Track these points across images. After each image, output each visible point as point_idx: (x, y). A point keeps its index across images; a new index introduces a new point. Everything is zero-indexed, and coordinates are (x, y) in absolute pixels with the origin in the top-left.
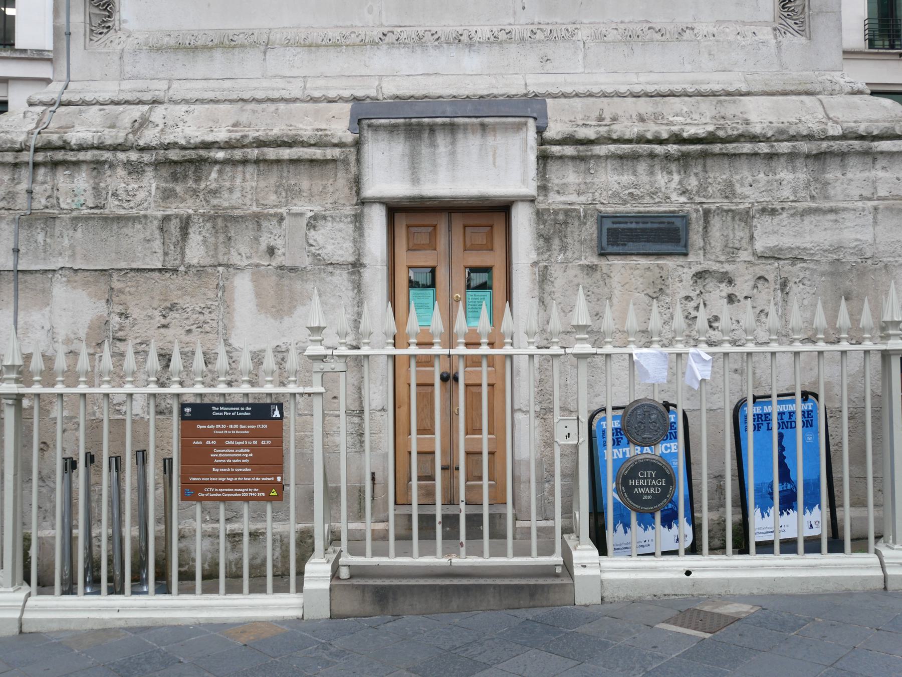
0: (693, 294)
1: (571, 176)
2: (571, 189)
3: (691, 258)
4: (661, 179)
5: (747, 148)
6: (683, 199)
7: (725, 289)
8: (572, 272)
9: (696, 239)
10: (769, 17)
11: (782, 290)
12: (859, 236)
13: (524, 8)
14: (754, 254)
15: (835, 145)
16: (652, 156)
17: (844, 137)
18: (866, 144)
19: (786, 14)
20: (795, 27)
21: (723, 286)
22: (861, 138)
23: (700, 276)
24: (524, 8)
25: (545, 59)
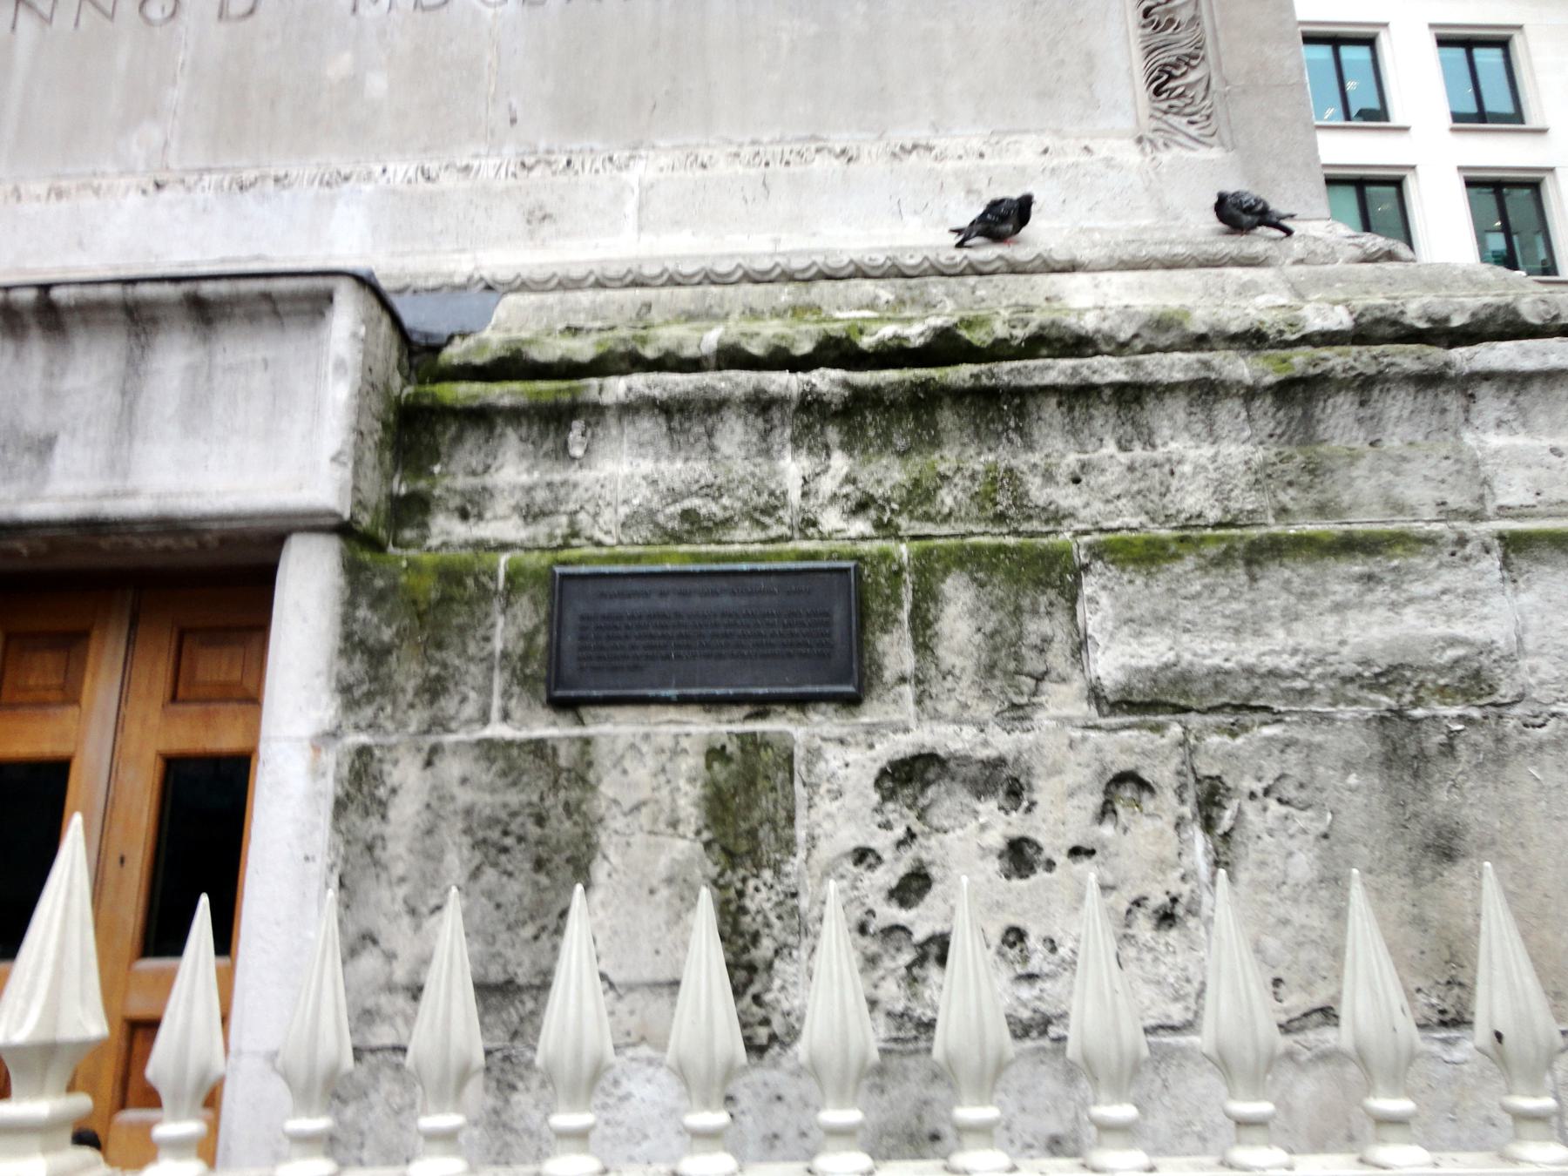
0: (882, 842)
1: (512, 469)
2: (502, 505)
3: (871, 713)
4: (792, 468)
5: (1058, 371)
6: (861, 526)
7: (995, 823)
8: (452, 768)
9: (895, 651)
10: (1127, 124)
11: (1208, 825)
12: (1460, 629)
13: (513, 121)
14: (1095, 694)
15: (1337, 359)
16: (761, 404)
17: (1361, 335)
18: (1436, 355)
19: (1164, 106)
20: (1192, 130)
21: (989, 807)
22: (1413, 336)
23: (908, 776)
24: (513, 121)
25: (539, 214)
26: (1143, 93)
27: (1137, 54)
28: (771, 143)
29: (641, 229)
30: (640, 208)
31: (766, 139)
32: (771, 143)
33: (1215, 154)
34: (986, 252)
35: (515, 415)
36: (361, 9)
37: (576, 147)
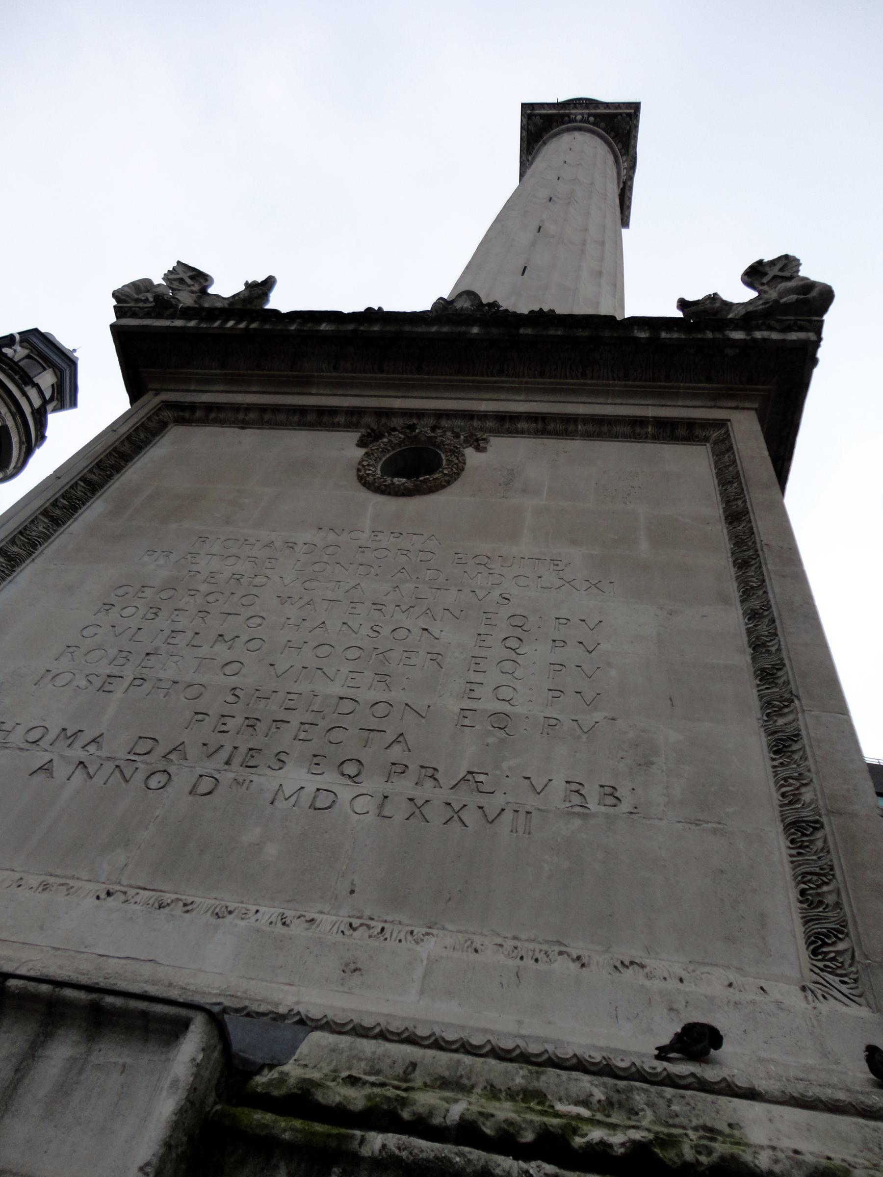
19: (820, 964)
20: (843, 988)
24: (352, 892)
25: (352, 967)
26: (804, 953)
27: (798, 922)
28: (527, 940)
29: (422, 992)
30: (425, 976)
31: (523, 937)
32: (527, 940)
33: (863, 1012)
34: (682, 1069)
35: (291, 1150)
36: (276, 803)
37: (389, 919)
